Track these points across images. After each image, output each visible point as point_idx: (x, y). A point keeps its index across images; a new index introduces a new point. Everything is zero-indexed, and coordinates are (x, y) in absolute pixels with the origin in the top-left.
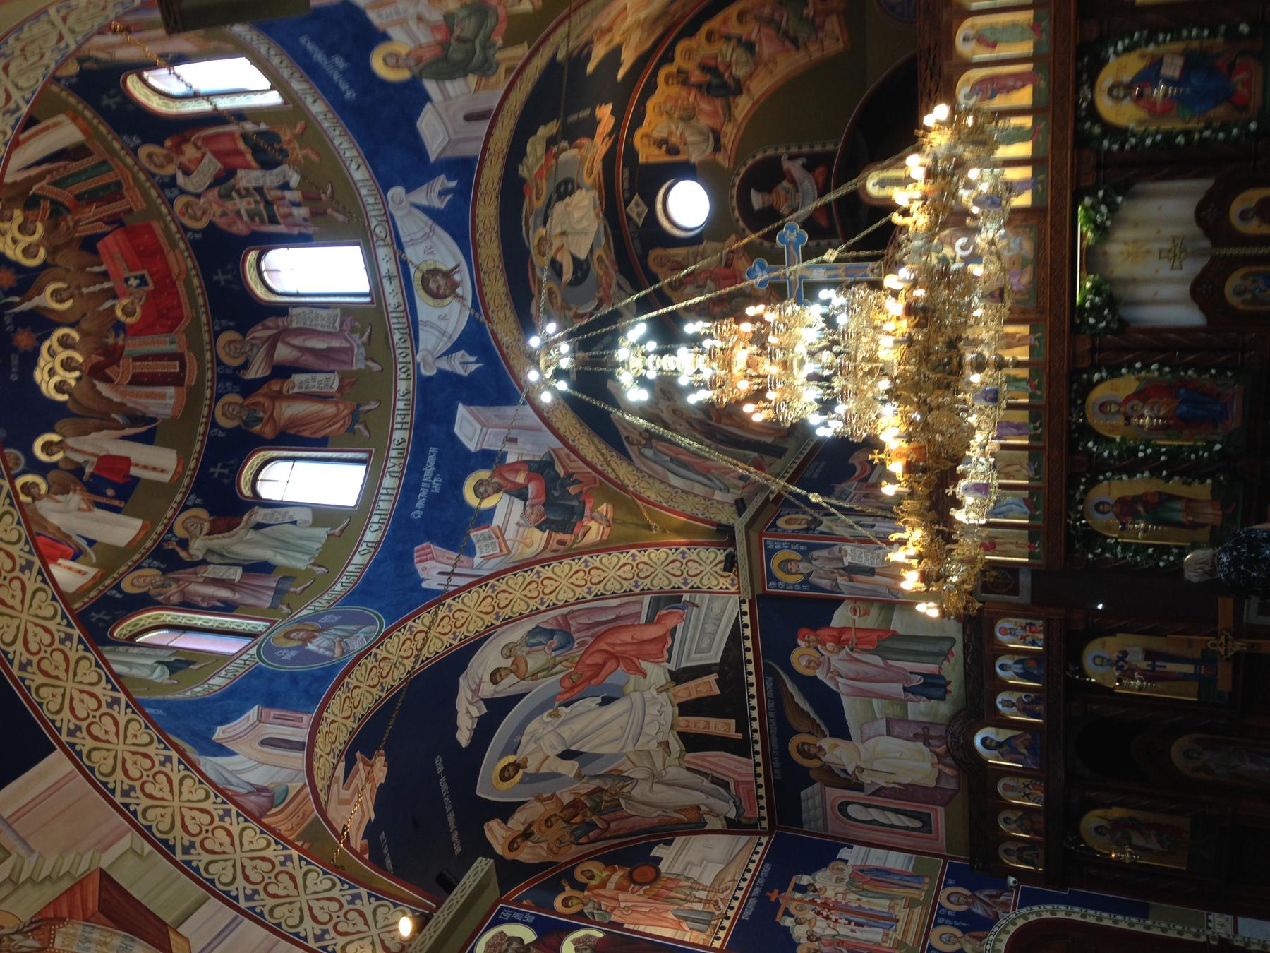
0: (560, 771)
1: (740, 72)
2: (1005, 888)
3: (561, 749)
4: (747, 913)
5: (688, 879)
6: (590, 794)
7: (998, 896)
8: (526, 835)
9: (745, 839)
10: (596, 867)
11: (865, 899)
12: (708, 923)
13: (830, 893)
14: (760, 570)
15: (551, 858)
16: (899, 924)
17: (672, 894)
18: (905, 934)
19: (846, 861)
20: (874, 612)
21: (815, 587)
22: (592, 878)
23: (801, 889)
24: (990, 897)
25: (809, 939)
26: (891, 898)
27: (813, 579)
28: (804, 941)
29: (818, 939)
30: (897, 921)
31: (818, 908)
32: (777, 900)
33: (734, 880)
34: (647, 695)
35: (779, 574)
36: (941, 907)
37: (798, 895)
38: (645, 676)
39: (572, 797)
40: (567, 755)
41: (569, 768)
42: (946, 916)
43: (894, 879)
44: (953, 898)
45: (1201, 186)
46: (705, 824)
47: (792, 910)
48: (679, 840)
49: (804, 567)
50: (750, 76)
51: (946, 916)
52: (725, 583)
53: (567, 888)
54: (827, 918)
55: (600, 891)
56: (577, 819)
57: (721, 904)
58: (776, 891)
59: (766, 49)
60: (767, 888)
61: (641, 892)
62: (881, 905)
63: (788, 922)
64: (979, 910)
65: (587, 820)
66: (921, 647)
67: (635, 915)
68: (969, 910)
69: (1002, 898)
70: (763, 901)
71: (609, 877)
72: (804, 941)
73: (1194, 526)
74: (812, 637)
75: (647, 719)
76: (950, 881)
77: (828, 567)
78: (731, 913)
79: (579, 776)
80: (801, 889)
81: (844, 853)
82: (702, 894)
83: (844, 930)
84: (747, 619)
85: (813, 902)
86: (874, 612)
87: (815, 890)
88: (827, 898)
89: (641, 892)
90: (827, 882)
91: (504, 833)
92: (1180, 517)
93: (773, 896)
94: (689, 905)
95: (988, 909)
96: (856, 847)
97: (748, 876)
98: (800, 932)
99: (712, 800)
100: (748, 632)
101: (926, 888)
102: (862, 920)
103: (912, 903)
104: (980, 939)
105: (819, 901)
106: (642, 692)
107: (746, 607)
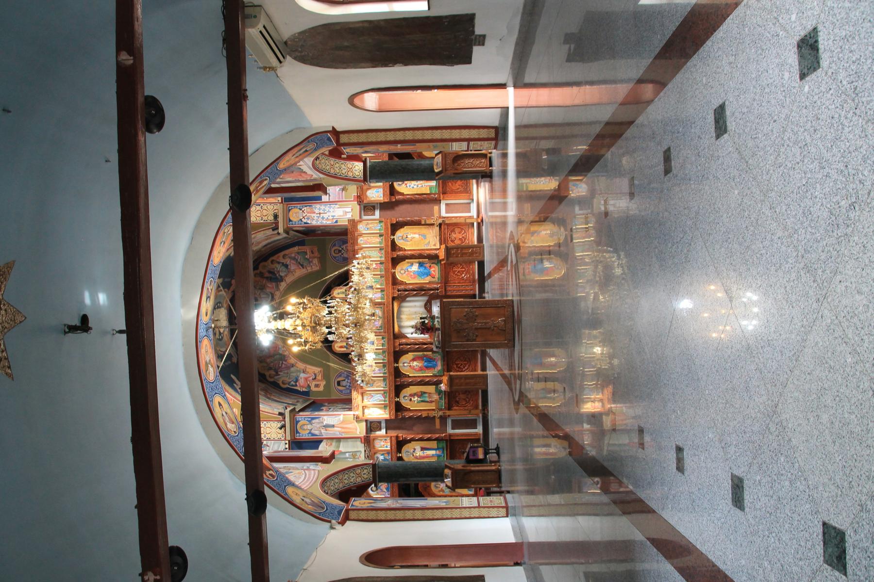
1: (282, 274)
14: (294, 430)
20: (334, 444)
21: (313, 435)
27: (313, 431)
35: (299, 430)
45: (425, 298)
49: (309, 427)
50: (286, 276)
52: (280, 436)
59: (293, 267)
73: (431, 402)
77: (318, 426)
86: (334, 444)
92: (427, 399)
107: (287, 446)
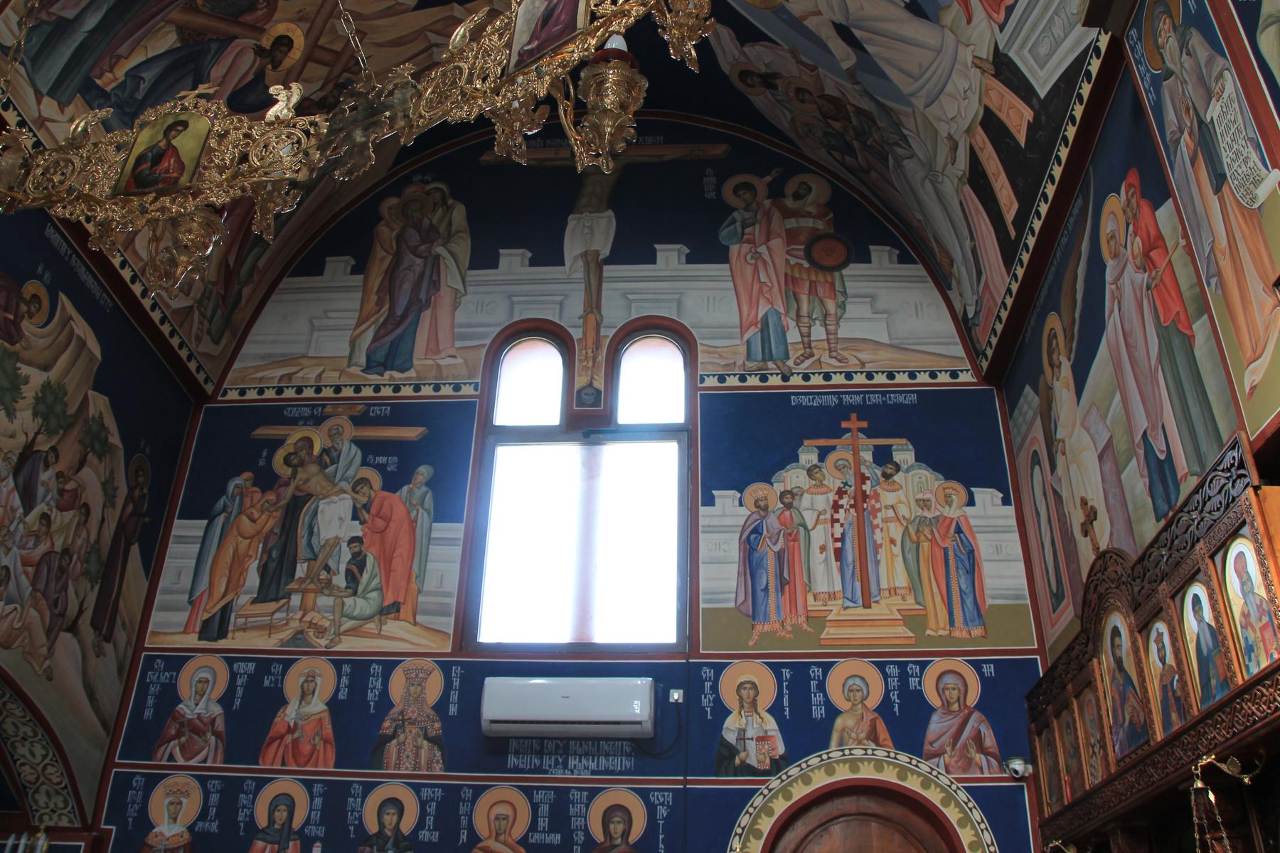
0: (831, 45)
2: (1003, 758)
3: (840, 19)
4: (805, 401)
5: (842, 306)
6: (859, 111)
7: (982, 749)
8: (769, 80)
9: (959, 351)
10: (819, 190)
11: (897, 550)
12: (767, 356)
13: (888, 498)
15: (792, 135)
16: (860, 612)
17: (804, 298)
18: (839, 623)
19: (971, 502)
22: (797, 196)
23: (883, 456)
24: (978, 738)
25: (783, 495)
26: (915, 586)
28: (778, 487)
29: (789, 506)
30: (867, 605)
31: (851, 490)
32: (848, 430)
33: (863, 364)
34: (961, 49)
36: (923, 665)
37: (868, 456)
38: (969, 21)
39: (835, 93)
40: (844, 32)
41: (845, 56)
42: (904, 677)
43: (960, 581)
44: (949, 680)
46: (950, 289)
47: (832, 458)
48: (918, 270)
51: (904, 677)
53: (768, 179)
54: (836, 507)
55: (776, 216)
56: (837, 125)
57: (808, 363)
58: (864, 424)
60: (863, 411)
61: (793, 261)
62: (892, 571)
63: (808, 456)
64: (937, 725)
65: (848, 138)
66: (1195, 411)
67: (749, 271)
68: (931, 710)
69: (979, 758)
70: (843, 411)
71: (809, 215)
72: (778, 487)
74: (1134, 201)
75: (949, 88)
76: (989, 670)
78: (796, 380)
79: (851, 74)
80: (883, 456)
81: (987, 497)
82: (818, 332)
83: (819, 536)
84: (1095, 66)
85: (864, 479)
87: (887, 476)
88: (877, 497)
89: (793, 261)
90: (913, 487)
91: (736, 53)
93: (853, 423)
94: (792, 324)
95: (946, 739)
96: (1010, 510)
97: (880, 379)
98: (793, 477)
99: (963, 269)
100: (1086, 89)
101: (957, 634)
102: (850, 555)
103: (914, 620)
104: (873, 736)
105: (867, 487)
106: (958, 41)
